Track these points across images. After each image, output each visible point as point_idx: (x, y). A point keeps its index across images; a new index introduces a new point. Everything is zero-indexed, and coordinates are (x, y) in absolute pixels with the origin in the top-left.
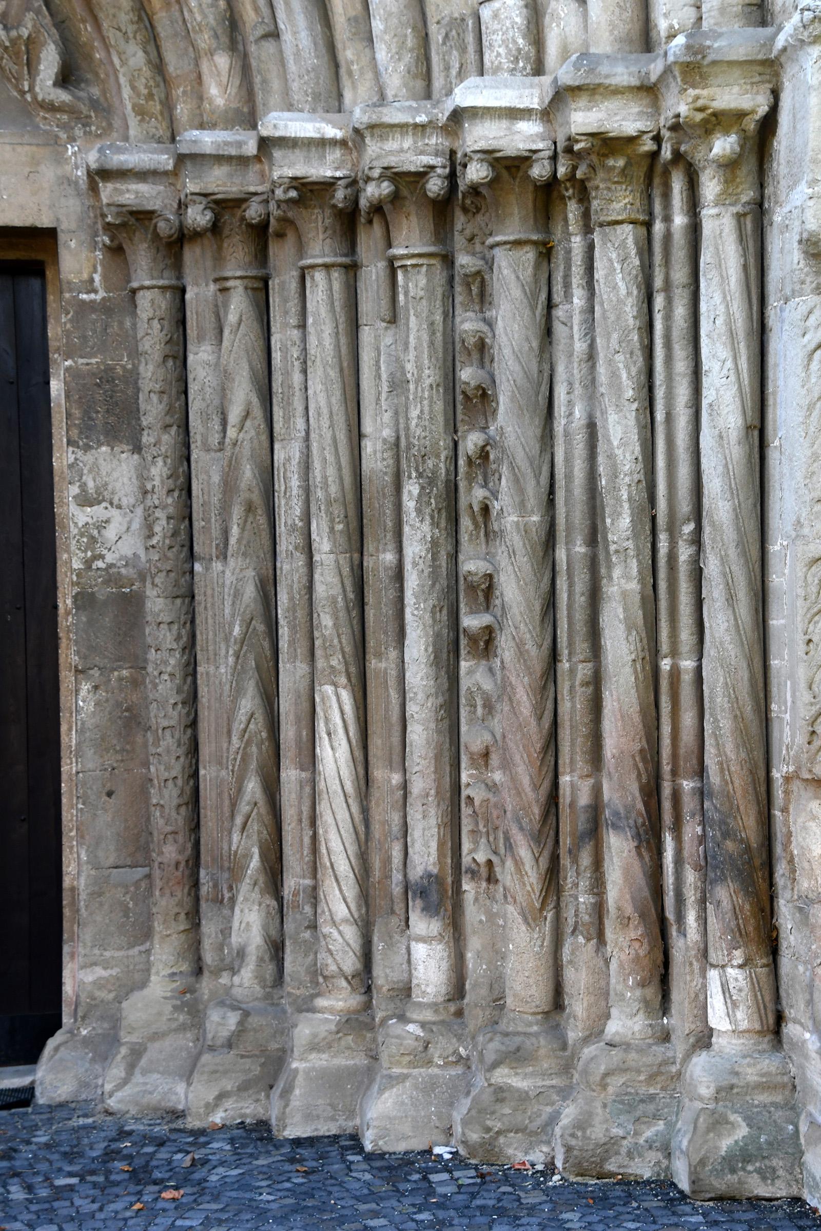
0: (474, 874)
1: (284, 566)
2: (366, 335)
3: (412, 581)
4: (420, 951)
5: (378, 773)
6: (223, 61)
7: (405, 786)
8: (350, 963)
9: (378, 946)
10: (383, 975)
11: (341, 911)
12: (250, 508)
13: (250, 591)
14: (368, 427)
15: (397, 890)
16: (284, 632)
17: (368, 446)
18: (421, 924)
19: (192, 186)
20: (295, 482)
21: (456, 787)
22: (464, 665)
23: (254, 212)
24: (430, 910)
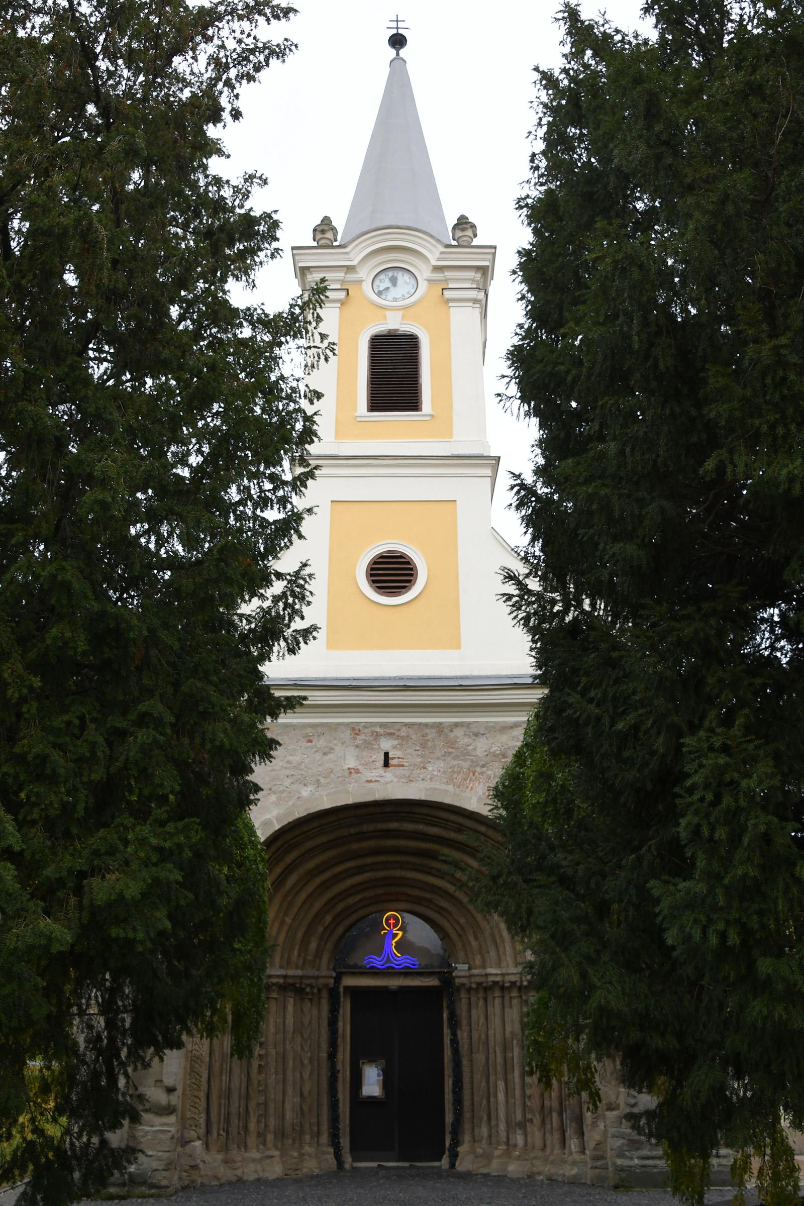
0: (528, 1121)
1: (490, 1055)
2: (506, 1010)
3: (515, 1060)
4: (518, 1137)
5: (510, 1100)
6: (479, 956)
7: (515, 1103)
8: (505, 1139)
9: (510, 1136)
10: (511, 1142)
11: (503, 1128)
12: (484, 1043)
13: (484, 1061)
14: (507, 1028)
15: (514, 1124)
16: (490, 1069)
17: (507, 1032)
18: (519, 1131)
19: (473, 980)
20: (493, 1038)
21: (525, 1103)
22: (526, 1078)
23: (484, 985)
24: (520, 1129)
